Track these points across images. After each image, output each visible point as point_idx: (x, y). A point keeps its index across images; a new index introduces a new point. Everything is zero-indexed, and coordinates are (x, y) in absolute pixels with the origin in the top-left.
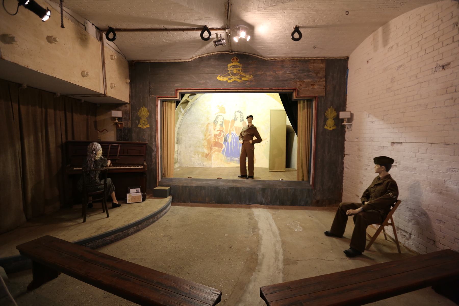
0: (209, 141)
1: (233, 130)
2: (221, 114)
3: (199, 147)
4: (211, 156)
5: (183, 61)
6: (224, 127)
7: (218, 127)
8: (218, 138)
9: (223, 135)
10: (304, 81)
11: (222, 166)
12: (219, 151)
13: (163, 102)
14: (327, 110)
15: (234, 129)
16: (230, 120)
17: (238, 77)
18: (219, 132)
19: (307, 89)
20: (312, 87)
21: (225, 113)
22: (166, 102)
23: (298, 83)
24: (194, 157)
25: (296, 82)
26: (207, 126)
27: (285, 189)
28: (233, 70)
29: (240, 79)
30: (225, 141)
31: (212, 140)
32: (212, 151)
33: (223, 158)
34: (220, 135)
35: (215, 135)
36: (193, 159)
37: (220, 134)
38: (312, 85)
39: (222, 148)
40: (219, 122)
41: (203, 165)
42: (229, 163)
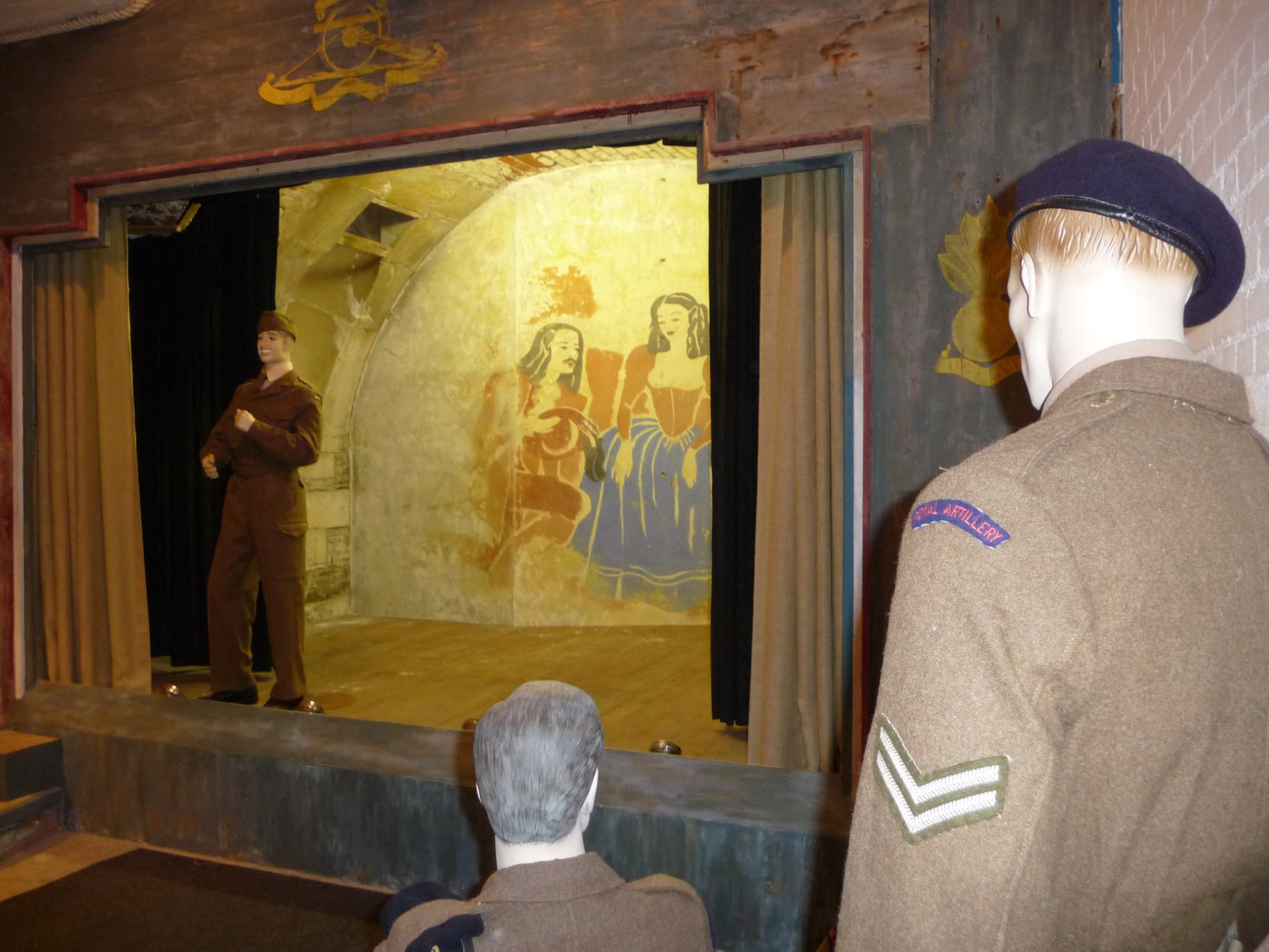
0: (496, 475)
1: (640, 408)
2: (565, 318)
3: (449, 506)
4: (507, 561)
5: (103, 19)
6: (584, 389)
7: (549, 395)
8: (547, 458)
9: (583, 439)
10: (771, 35)
11: (574, 618)
12: (557, 533)
13: (29, 255)
14: (952, 226)
15: (649, 404)
16: (626, 353)
17: (365, 68)
18: (556, 420)
19: (792, 85)
20: (826, 67)
21: (589, 308)
22: (52, 258)
23: (729, 55)
24: (424, 565)
25: (713, 48)
26: (489, 388)
27: (663, 820)
28: (338, 32)
29: (378, 77)
30: (596, 471)
31: (514, 469)
32: (516, 533)
33: (583, 573)
34: (563, 443)
35: (528, 440)
36: (419, 572)
37: (560, 434)
38: (825, 51)
39: (572, 510)
40: (558, 366)
41: (471, 610)
42: (618, 606)
